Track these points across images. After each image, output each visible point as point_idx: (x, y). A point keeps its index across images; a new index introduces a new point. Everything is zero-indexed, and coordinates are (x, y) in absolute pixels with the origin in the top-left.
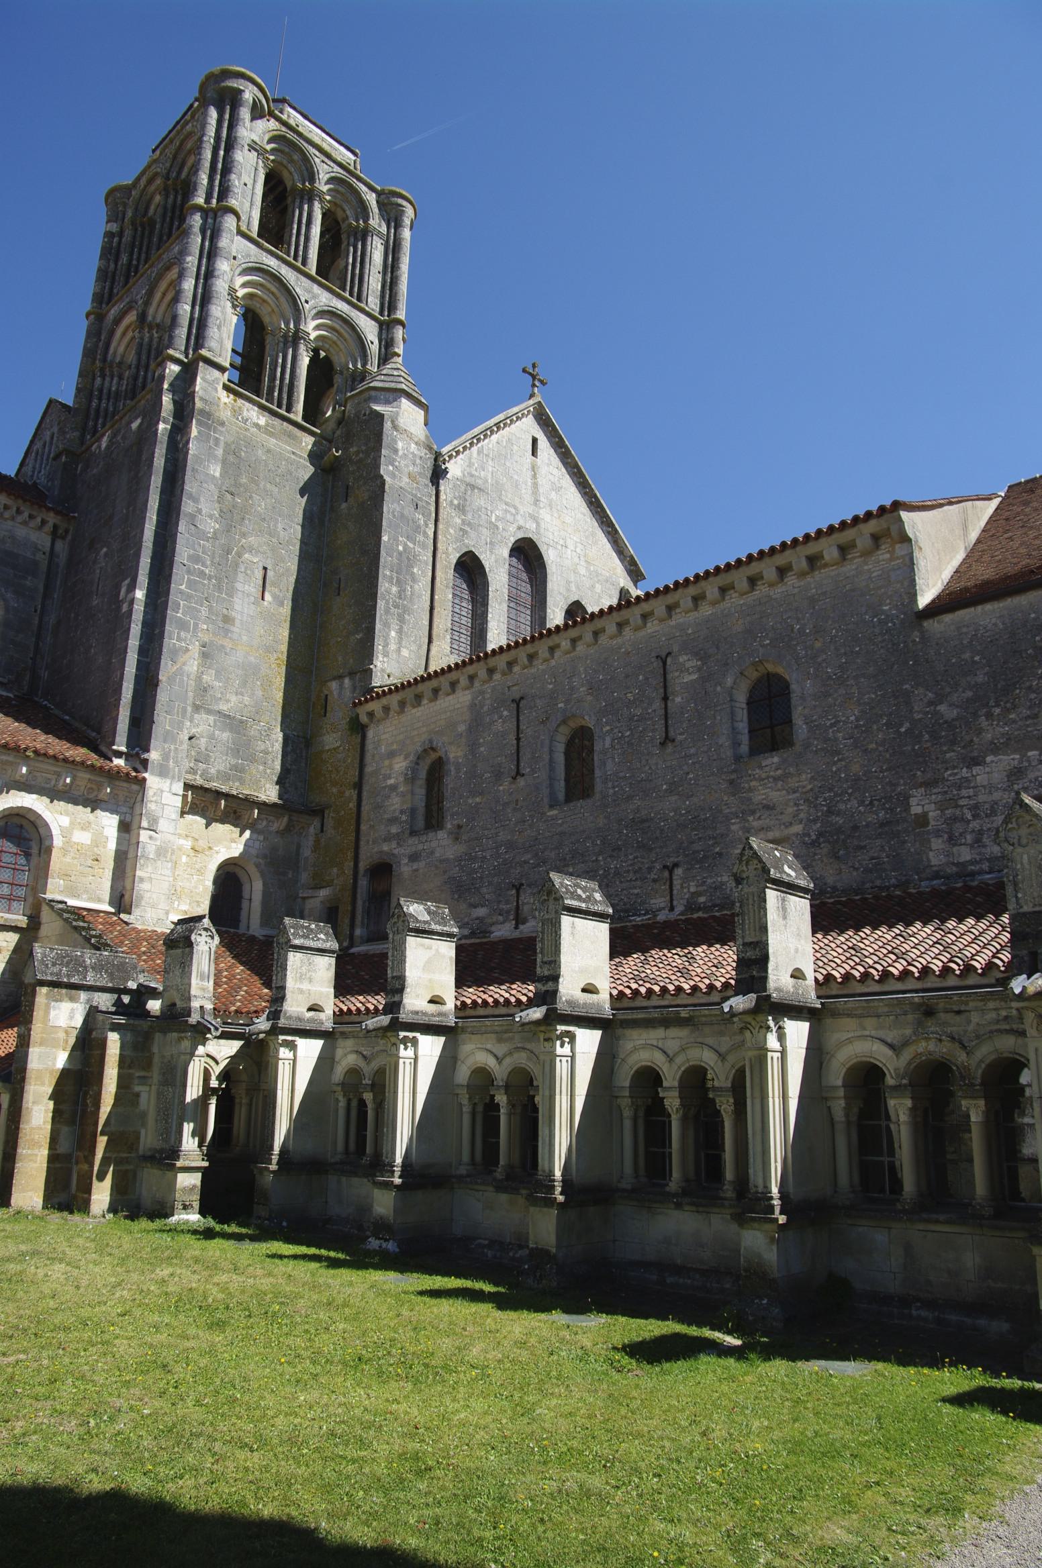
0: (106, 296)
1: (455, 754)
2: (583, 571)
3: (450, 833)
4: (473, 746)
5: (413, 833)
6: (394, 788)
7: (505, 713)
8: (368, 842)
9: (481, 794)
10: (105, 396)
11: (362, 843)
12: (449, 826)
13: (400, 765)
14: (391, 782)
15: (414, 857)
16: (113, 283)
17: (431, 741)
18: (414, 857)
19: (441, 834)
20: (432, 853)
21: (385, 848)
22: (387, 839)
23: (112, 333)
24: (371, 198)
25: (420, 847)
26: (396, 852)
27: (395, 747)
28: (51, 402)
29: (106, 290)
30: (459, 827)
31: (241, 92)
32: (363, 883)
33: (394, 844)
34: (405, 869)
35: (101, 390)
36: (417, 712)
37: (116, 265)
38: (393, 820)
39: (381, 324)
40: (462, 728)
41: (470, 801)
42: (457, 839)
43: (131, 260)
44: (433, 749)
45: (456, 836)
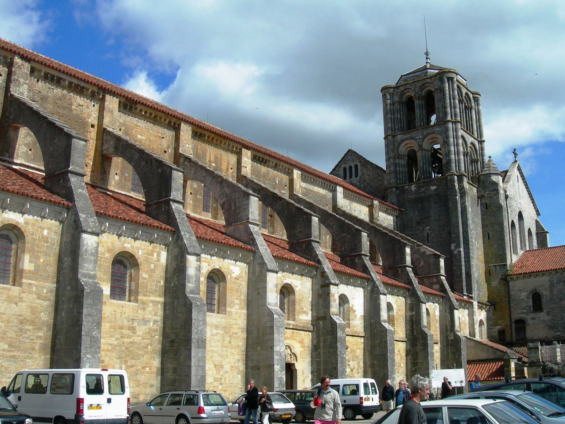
0: (393, 128)
1: (545, 293)
2: (529, 218)
3: (545, 313)
4: (551, 291)
5: (531, 312)
6: (523, 300)
7: (562, 284)
8: (514, 314)
9: (556, 304)
10: (400, 166)
11: (512, 314)
12: (545, 311)
13: (524, 294)
14: (522, 298)
15: (533, 319)
16: (394, 123)
17: (535, 288)
18: (533, 319)
19: (542, 313)
20: (540, 318)
21: (522, 316)
22: (522, 313)
23: (400, 144)
24: (471, 96)
25: (534, 316)
26: (526, 317)
27: (521, 288)
28: (349, 150)
29: (393, 127)
30: (549, 312)
31: (454, 78)
32: (514, 324)
33: (525, 315)
34: (530, 322)
35: (399, 164)
36: (530, 280)
37: (394, 116)
38: (525, 308)
39: (479, 141)
40: (547, 286)
41: (552, 305)
42: (548, 315)
43: (401, 116)
44: (536, 290)
45: (548, 314)
